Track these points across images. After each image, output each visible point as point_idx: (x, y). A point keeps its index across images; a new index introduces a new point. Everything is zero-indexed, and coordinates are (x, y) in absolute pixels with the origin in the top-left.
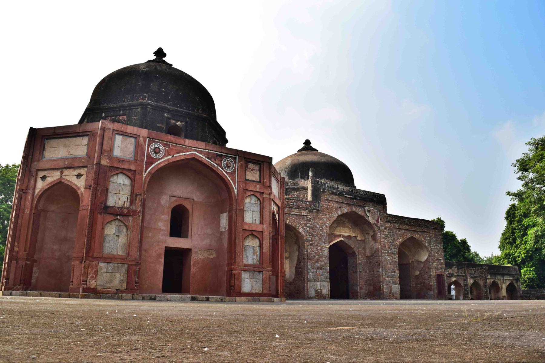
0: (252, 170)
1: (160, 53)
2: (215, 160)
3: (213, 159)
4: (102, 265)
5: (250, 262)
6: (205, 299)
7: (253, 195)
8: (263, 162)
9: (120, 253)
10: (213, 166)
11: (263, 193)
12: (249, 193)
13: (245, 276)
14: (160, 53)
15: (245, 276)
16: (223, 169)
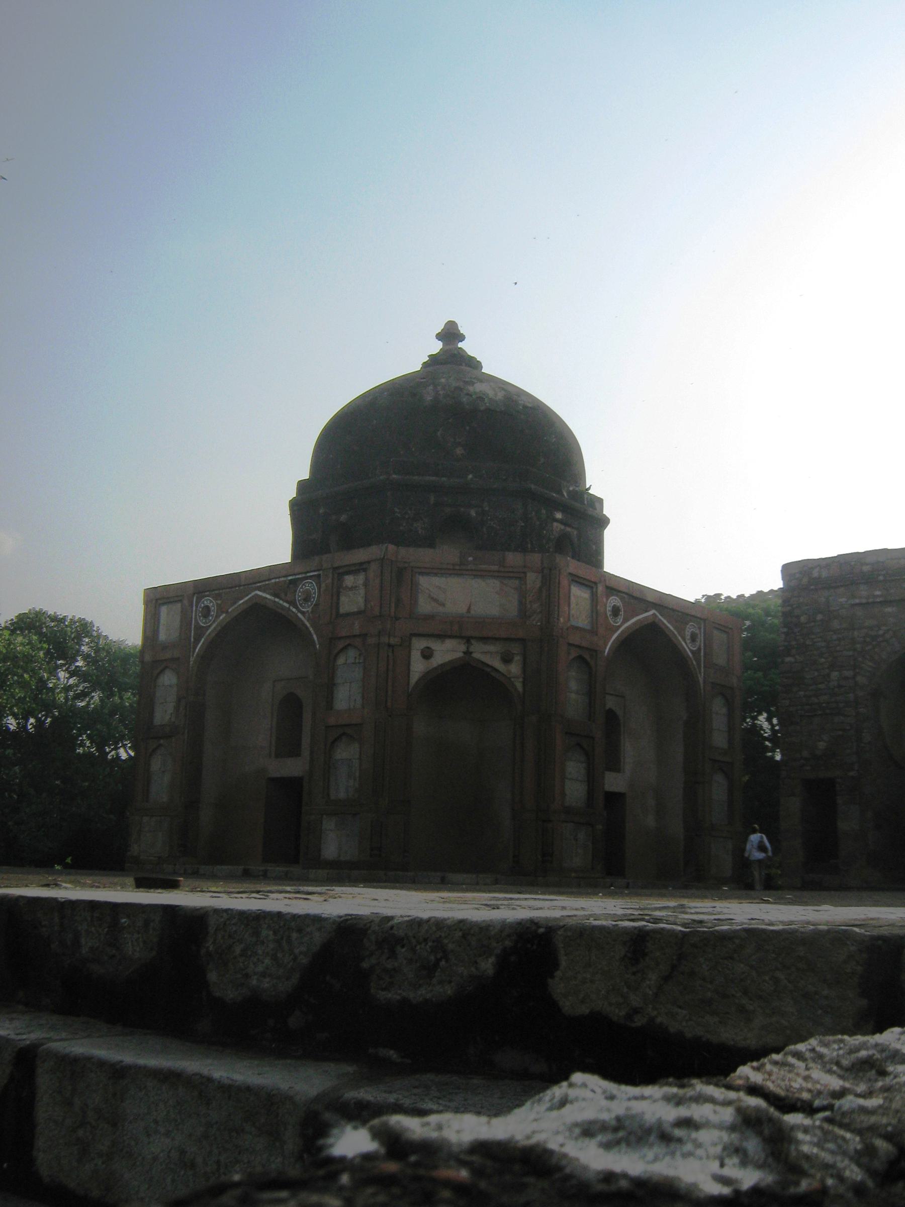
0: (351, 589)
1: (450, 334)
2: (286, 595)
3: (283, 595)
4: (145, 819)
5: (342, 795)
6: (261, 873)
7: (349, 645)
8: (369, 562)
9: (165, 800)
10: (283, 608)
11: (366, 635)
12: (341, 644)
13: (329, 825)
14: (450, 334)
15: (329, 825)
16: (297, 608)
